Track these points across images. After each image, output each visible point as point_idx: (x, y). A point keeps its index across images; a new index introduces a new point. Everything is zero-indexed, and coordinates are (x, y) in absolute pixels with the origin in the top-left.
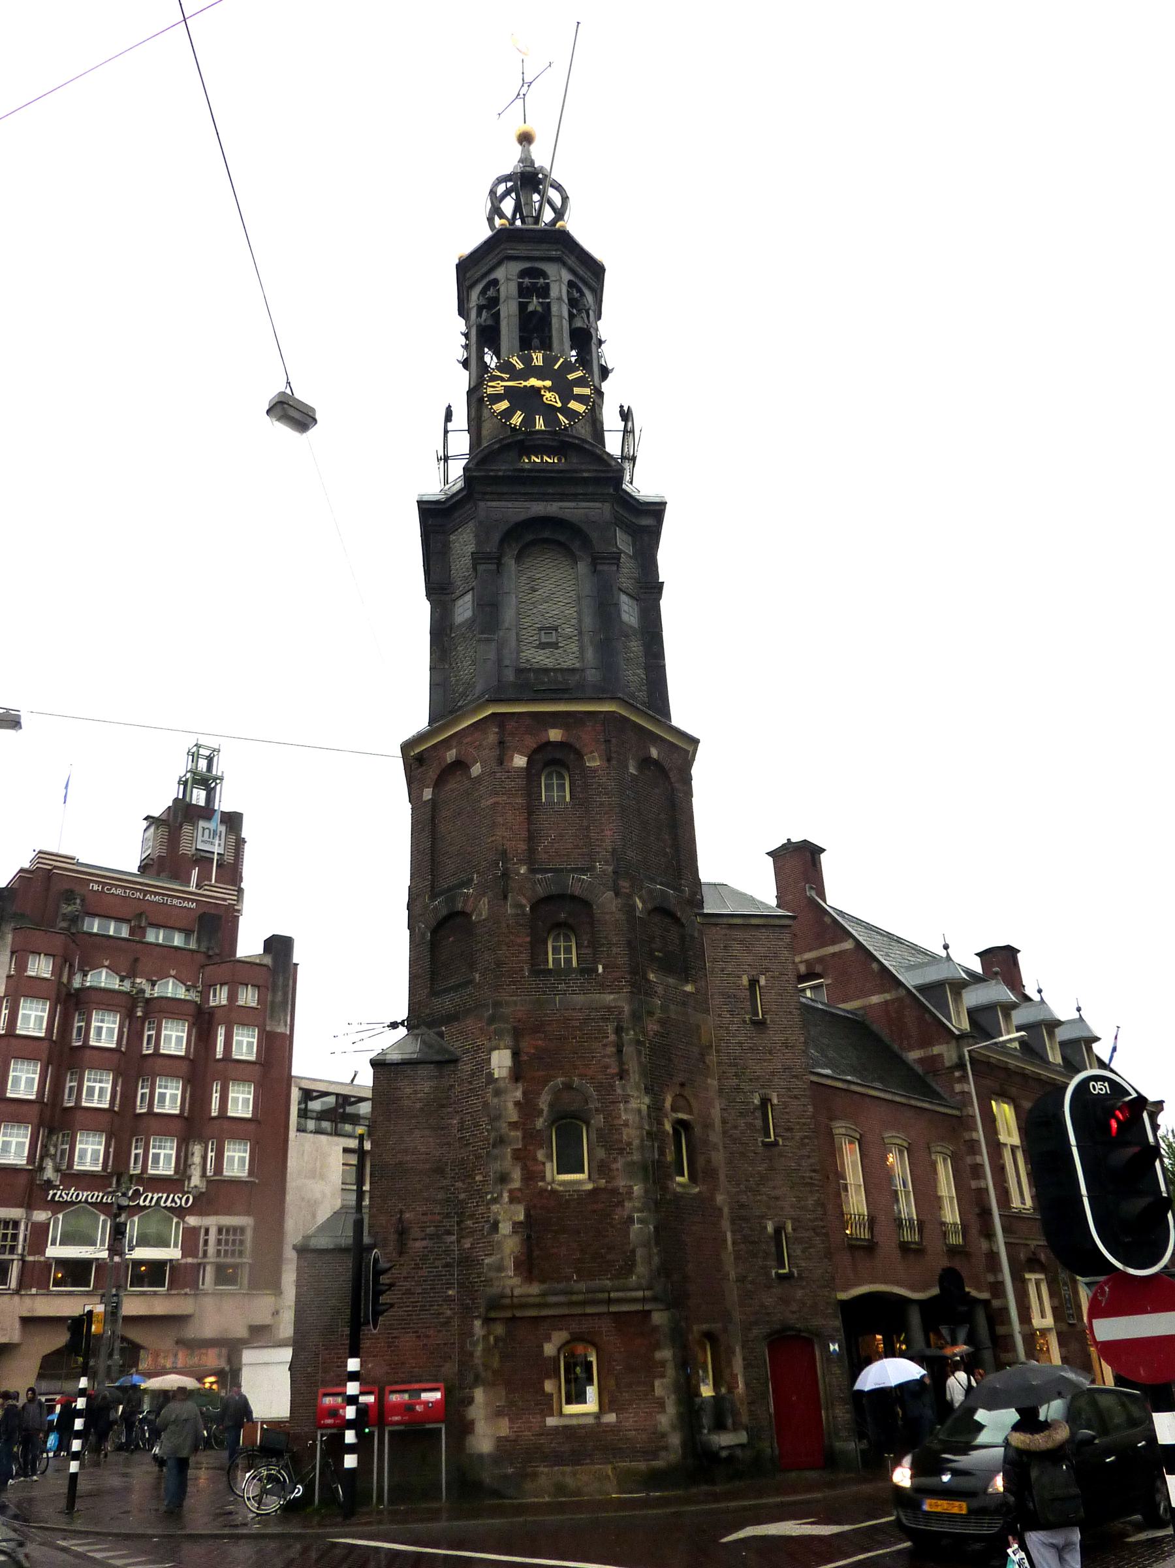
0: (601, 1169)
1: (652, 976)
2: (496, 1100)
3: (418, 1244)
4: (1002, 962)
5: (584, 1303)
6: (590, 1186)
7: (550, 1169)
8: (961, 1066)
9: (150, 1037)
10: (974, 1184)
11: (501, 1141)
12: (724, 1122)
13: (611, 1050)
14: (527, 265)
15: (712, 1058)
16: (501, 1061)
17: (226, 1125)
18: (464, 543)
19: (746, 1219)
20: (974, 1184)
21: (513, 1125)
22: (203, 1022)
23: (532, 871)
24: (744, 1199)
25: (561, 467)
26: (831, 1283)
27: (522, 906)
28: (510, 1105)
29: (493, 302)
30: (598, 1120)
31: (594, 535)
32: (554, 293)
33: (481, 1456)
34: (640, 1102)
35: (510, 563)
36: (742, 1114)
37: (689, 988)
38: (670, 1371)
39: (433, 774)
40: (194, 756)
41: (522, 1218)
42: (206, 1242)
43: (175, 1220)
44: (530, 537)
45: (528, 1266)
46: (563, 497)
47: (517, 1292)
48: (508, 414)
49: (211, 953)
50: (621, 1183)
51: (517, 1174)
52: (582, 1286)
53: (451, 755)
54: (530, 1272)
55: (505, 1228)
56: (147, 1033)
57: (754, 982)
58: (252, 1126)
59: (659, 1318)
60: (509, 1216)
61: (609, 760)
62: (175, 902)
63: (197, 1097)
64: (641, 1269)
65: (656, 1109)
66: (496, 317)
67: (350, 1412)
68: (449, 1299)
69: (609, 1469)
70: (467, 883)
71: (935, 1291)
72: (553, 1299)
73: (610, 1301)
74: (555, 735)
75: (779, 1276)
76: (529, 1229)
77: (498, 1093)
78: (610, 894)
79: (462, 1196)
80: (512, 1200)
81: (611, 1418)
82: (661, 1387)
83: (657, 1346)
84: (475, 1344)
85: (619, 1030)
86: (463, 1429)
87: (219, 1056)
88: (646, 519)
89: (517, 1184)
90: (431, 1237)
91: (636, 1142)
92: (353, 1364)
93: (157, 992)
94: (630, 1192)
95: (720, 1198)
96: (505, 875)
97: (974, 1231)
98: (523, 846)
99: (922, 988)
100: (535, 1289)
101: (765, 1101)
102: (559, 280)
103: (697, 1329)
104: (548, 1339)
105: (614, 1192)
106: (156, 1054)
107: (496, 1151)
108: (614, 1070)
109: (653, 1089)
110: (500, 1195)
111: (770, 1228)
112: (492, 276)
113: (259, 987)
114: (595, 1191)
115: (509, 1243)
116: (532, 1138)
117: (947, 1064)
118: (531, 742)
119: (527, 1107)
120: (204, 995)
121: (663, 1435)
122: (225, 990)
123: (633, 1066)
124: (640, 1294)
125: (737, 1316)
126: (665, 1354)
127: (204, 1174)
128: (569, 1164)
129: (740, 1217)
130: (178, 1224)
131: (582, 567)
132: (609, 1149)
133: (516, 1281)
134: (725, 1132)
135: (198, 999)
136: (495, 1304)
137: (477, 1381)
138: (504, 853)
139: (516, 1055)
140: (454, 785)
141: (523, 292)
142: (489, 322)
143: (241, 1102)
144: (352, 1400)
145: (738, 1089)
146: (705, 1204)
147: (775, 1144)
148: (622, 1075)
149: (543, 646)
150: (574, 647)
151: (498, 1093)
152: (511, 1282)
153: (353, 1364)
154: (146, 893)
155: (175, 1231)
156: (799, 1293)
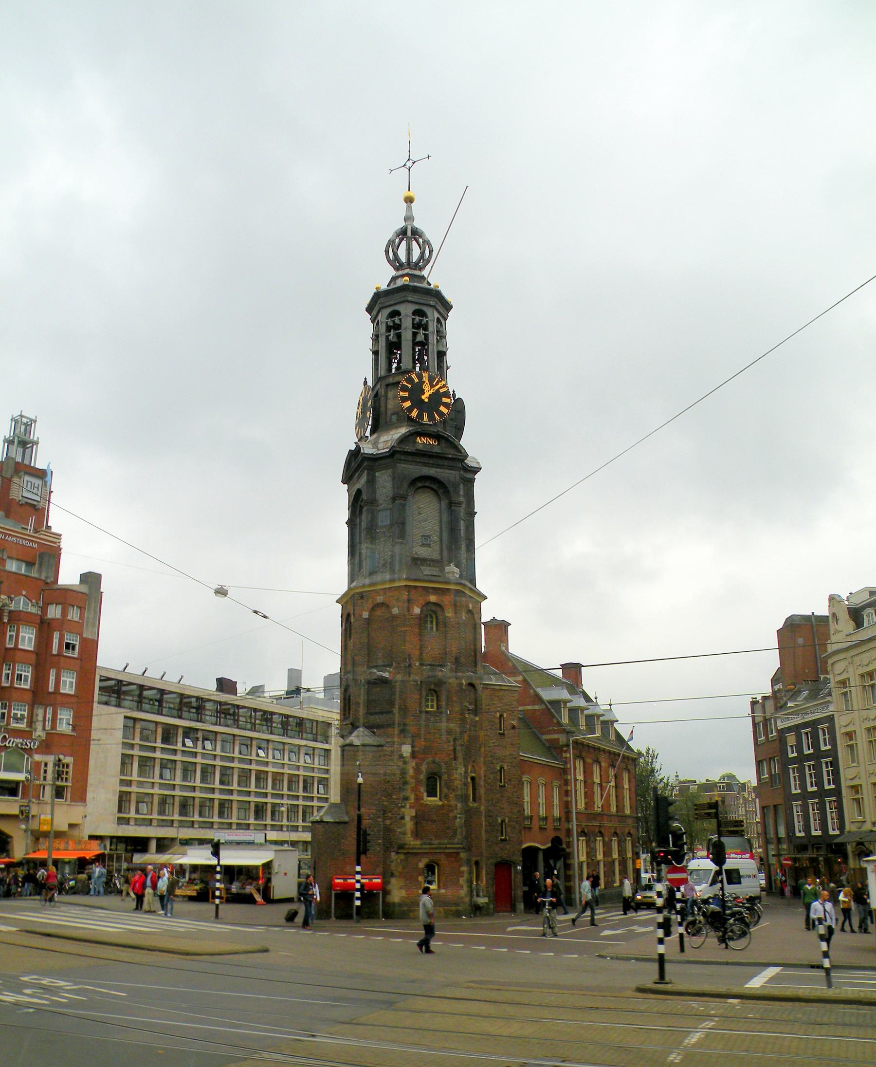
1: (467, 715)
4: (573, 670)
5: (436, 848)
6: (441, 803)
7: (425, 794)
8: (568, 745)
9: (11, 636)
10: (565, 799)
11: (405, 783)
12: (485, 776)
14: (417, 307)
15: (482, 750)
16: (406, 750)
17: (59, 699)
18: (385, 482)
19: (490, 816)
20: (565, 799)
21: (412, 777)
22: (45, 627)
23: (422, 665)
24: (490, 808)
25: (437, 450)
26: (521, 843)
29: (397, 327)
30: (445, 777)
31: (451, 489)
32: (430, 329)
33: (394, 904)
34: (462, 770)
35: (410, 498)
36: (492, 773)
37: (477, 719)
38: (466, 875)
39: (369, 605)
40: (16, 421)
41: (414, 814)
42: (45, 771)
43: (26, 756)
44: (420, 485)
45: (416, 834)
46: (438, 466)
48: (404, 399)
49: (49, 581)
50: (453, 803)
52: (437, 842)
53: (380, 599)
55: (407, 818)
56: (8, 634)
57: (501, 716)
58: (74, 700)
59: (463, 855)
60: (409, 813)
61: (456, 613)
62: (25, 542)
63: (40, 680)
64: (459, 836)
65: (466, 772)
66: (399, 336)
67: (358, 886)
68: (379, 844)
69: (441, 909)
71: (549, 845)
72: (424, 846)
73: (446, 848)
74: (433, 598)
75: (502, 840)
76: (418, 820)
77: (405, 763)
79: (385, 803)
81: (443, 891)
82: (462, 881)
83: (461, 866)
84: (392, 862)
85: (455, 740)
86: (386, 893)
87: (55, 652)
88: (469, 474)
89: (412, 801)
91: (459, 787)
92: (358, 868)
93: (12, 607)
94: (456, 806)
95: (482, 808)
96: (410, 666)
97: (563, 819)
98: (417, 653)
99: (552, 702)
100: (418, 842)
101: (502, 768)
102: (433, 315)
103: (474, 859)
104: (420, 861)
105: (450, 806)
106: (16, 648)
108: (452, 756)
109: (466, 766)
111: (499, 821)
112: (397, 308)
113: (80, 608)
114: (443, 805)
115: (409, 825)
116: (418, 782)
117: (561, 743)
118: (422, 601)
119: (417, 770)
120: (44, 610)
121: (462, 898)
122: (59, 607)
123: (460, 756)
125: (484, 854)
127: (44, 729)
128: (432, 793)
129: (489, 815)
130: (28, 759)
131: (444, 503)
132: (448, 788)
133: (412, 839)
134: (485, 780)
135: (40, 613)
137: (392, 875)
138: (409, 655)
139: (413, 747)
140: (379, 612)
141: (417, 326)
142: (395, 340)
143: (68, 684)
144: (358, 881)
145: (492, 763)
146: (477, 811)
147: (504, 786)
148: (455, 759)
149: (423, 545)
150: (437, 548)
151: (405, 763)
152: (411, 841)
153: (358, 868)
154: (6, 535)
155: (27, 762)
156: (508, 847)
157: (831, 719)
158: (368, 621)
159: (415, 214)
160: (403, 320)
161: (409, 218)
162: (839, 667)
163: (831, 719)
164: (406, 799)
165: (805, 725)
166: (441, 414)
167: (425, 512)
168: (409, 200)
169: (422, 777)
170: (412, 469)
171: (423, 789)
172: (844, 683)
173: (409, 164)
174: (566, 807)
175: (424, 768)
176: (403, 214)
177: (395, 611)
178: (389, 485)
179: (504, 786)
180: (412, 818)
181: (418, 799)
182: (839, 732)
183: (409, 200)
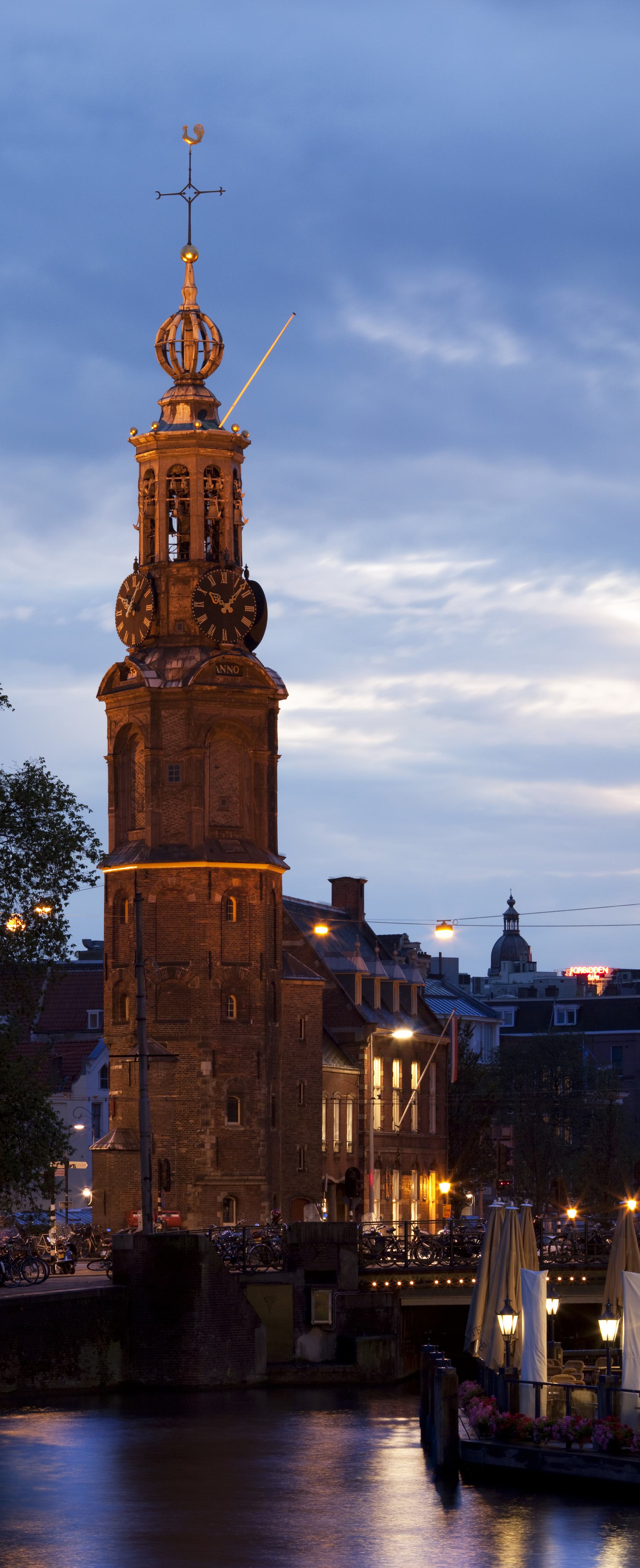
0: (246, 1122)
2: (204, 1086)
3: (160, 1149)
6: (242, 1129)
7: (226, 1118)
13: (254, 1064)
16: (206, 1067)
23: (223, 964)
27: (217, 984)
28: (211, 1089)
41: (214, 1141)
45: (218, 1162)
47: (212, 1174)
51: (213, 1122)
54: (217, 1165)
55: (208, 1146)
59: (262, 1187)
60: (209, 1140)
61: (261, 899)
65: (269, 1092)
70: (186, 964)
72: (225, 1178)
74: (236, 882)
76: (218, 1148)
78: (258, 980)
79: (180, 1128)
80: (211, 1133)
85: (258, 1054)
89: (212, 1127)
90: (165, 1146)
91: (263, 1109)
94: (259, 1133)
96: (210, 967)
98: (219, 950)
100: (219, 1173)
107: (204, 1110)
108: (255, 1074)
110: (205, 1131)
115: (210, 1154)
119: (217, 1089)
124: (260, 1178)
126: (266, 1204)
133: (212, 1170)
136: (200, 1178)
138: (210, 953)
148: (259, 1077)
151: (205, 1082)
160: (192, 483)
164: (207, 1123)
166: (242, 627)
169: (223, 1098)
171: (223, 1113)
173: (190, 194)
175: (225, 1088)
177: (192, 898)
179: (304, 1106)
180: (212, 1146)
181: (218, 1123)
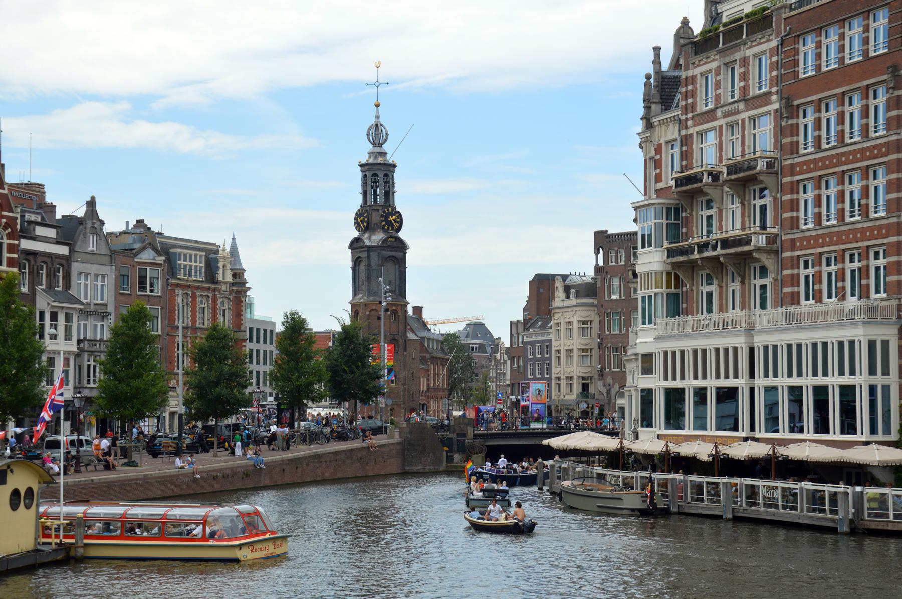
53: (374, 307)
140: (373, 312)
157: (550, 341)
158: (369, 316)
159: (381, 114)
161: (378, 117)
162: (556, 316)
163: (550, 341)
165: (538, 342)
167: (390, 269)
168: (377, 105)
170: (380, 249)
172: (558, 324)
174: (428, 385)
176: (374, 113)
178: (376, 259)
182: (554, 349)
183: (377, 105)
